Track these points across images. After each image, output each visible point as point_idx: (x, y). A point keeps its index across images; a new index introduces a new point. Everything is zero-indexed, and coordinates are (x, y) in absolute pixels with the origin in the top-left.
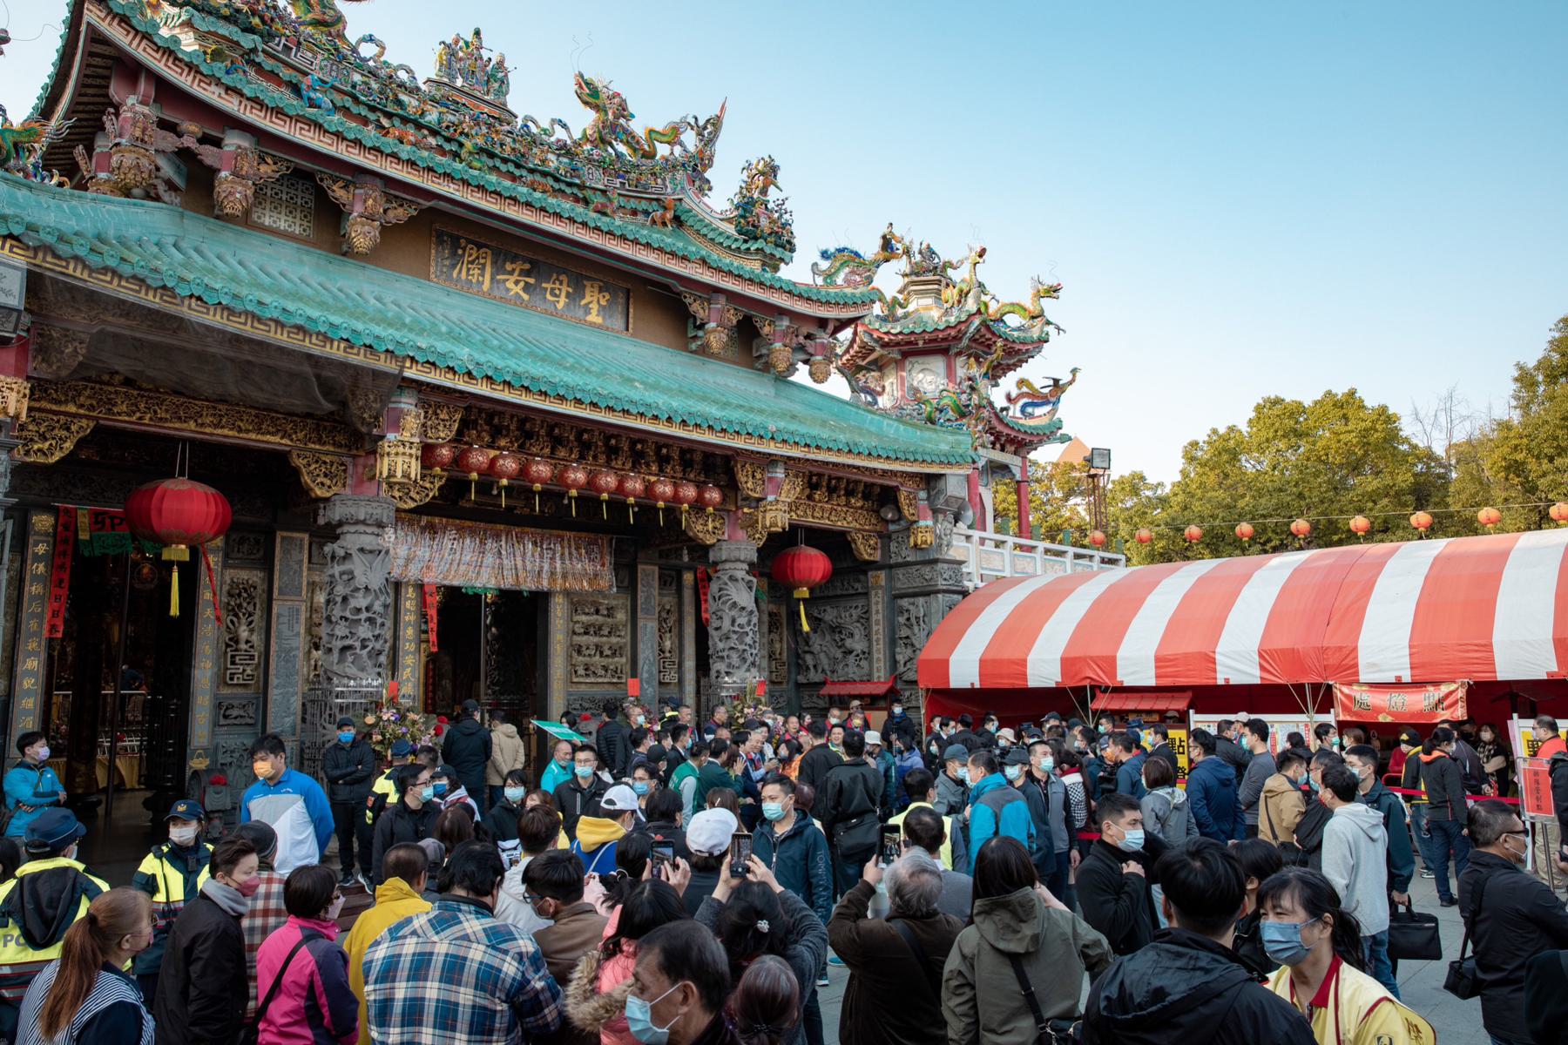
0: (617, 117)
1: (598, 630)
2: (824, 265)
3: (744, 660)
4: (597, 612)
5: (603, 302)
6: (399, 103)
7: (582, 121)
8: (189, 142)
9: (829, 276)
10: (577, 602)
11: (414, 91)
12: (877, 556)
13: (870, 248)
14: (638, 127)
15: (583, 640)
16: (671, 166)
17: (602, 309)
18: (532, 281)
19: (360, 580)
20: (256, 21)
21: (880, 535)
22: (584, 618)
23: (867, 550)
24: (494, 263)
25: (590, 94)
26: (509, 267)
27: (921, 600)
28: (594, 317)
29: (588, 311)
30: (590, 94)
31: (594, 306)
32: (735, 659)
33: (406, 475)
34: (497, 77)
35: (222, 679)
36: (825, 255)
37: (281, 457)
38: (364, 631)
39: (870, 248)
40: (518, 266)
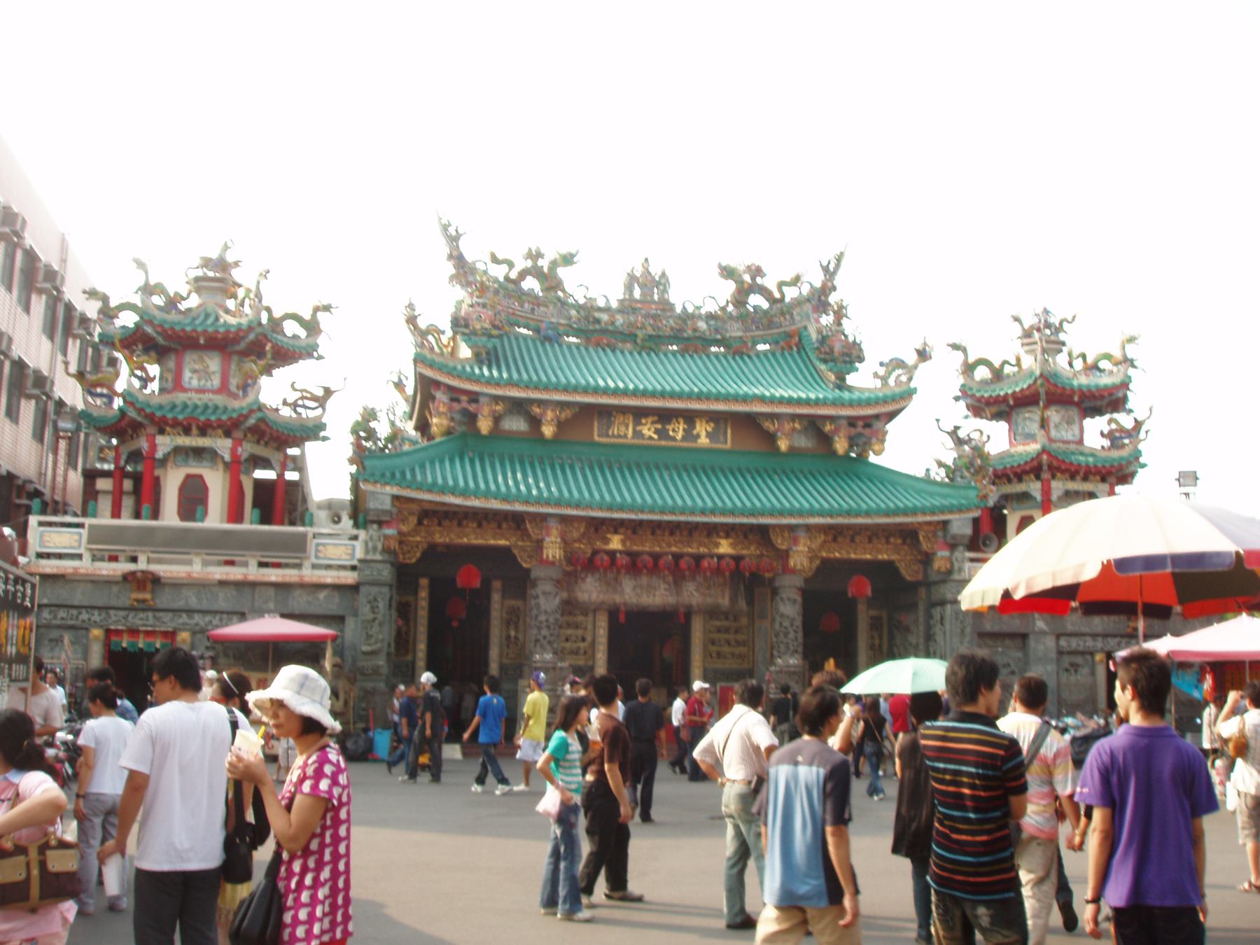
0: (753, 279)
1: (727, 630)
2: (882, 371)
3: (788, 648)
4: (727, 618)
5: (709, 429)
6: (598, 321)
7: (728, 289)
8: (465, 405)
9: (884, 379)
10: (712, 613)
11: (607, 310)
12: (920, 577)
13: (911, 359)
14: (770, 282)
15: (716, 636)
16: (798, 302)
17: (708, 435)
18: (659, 426)
19: (543, 607)
20: (495, 332)
21: (921, 562)
22: (718, 623)
23: (909, 572)
24: (635, 420)
25: (728, 272)
26: (644, 421)
27: (939, 609)
28: (704, 441)
29: (698, 436)
30: (728, 272)
31: (703, 434)
32: (782, 648)
33: (554, 557)
34: (662, 283)
35: (501, 656)
36: (881, 364)
37: (507, 551)
38: (545, 632)
39: (911, 359)
40: (650, 419)
